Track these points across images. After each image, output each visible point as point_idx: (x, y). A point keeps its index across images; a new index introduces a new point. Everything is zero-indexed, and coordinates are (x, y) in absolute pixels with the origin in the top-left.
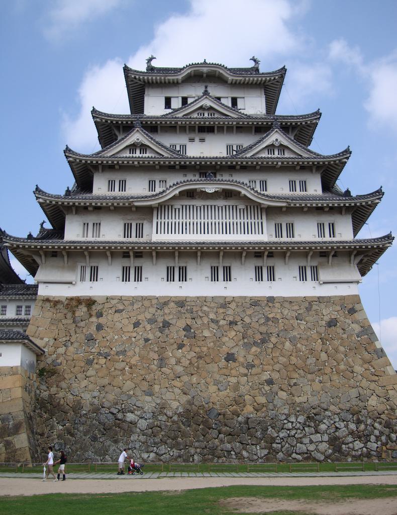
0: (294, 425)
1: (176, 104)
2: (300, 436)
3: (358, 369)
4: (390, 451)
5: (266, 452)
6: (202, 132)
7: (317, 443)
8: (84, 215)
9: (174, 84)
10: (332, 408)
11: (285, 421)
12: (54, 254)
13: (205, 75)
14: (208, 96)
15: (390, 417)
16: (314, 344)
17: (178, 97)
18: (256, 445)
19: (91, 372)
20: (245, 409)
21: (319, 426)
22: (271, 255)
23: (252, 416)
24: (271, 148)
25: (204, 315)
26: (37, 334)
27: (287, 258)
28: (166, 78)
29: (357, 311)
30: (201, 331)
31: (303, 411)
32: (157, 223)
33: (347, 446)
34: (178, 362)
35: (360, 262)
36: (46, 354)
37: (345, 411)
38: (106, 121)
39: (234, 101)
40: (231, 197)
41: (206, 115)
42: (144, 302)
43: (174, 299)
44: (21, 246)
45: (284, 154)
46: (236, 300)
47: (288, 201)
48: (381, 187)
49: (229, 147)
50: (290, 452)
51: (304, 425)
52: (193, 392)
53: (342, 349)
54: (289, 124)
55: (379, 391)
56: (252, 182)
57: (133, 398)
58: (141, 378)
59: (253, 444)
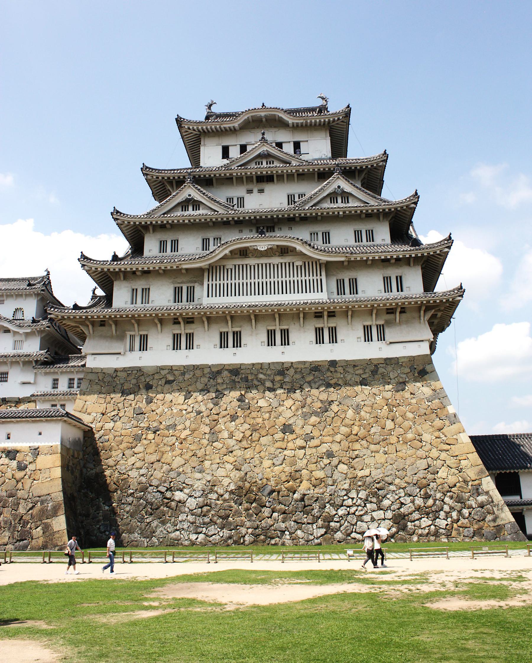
0: (355, 501)
1: (234, 152)
2: (362, 513)
3: (426, 437)
4: (461, 529)
5: (323, 531)
6: (261, 182)
7: (379, 521)
8: (132, 280)
9: (232, 132)
10: (397, 481)
11: (345, 498)
12: (102, 323)
13: (264, 120)
14: (265, 144)
15: (462, 490)
16: (380, 411)
17: (236, 145)
18: (312, 524)
19: (139, 448)
20: (302, 484)
21: (382, 501)
22: (332, 314)
23: (309, 492)
24: (333, 197)
25: (260, 384)
26: (84, 409)
27: (349, 317)
28: (222, 126)
29: (428, 373)
30: (256, 401)
31: (364, 485)
32: (208, 285)
33: (413, 524)
34: (231, 436)
35: (434, 316)
36: (94, 430)
37: (411, 485)
38: (157, 178)
39: (297, 146)
40: (288, 253)
41: (264, 163)
42: (195, 372)
43: (227, 367)
44: (66, 317)
45: (348, 202)
46: (295, 366)
47: (347, 255)
48: (450, 234)
49: (291, 199)
50: (349, 531)
51: (366, 501)
52: (245, 468)
53: (410, 415)
54: (353, 168)
55: (451, 461)
56: (314, 234)
57: (182, 475)
58: (191, 454)
59: (308, 523)
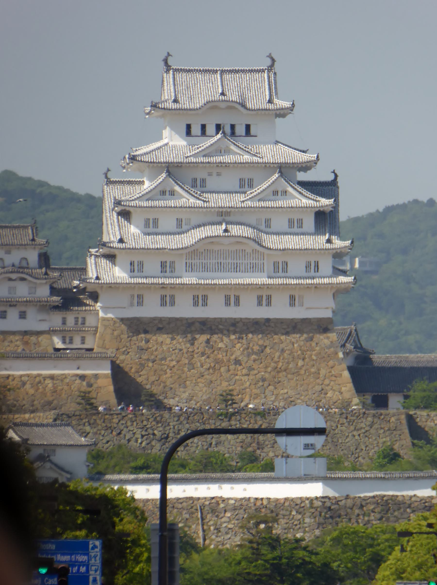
32: (186, 263)
55: (336, 387)
